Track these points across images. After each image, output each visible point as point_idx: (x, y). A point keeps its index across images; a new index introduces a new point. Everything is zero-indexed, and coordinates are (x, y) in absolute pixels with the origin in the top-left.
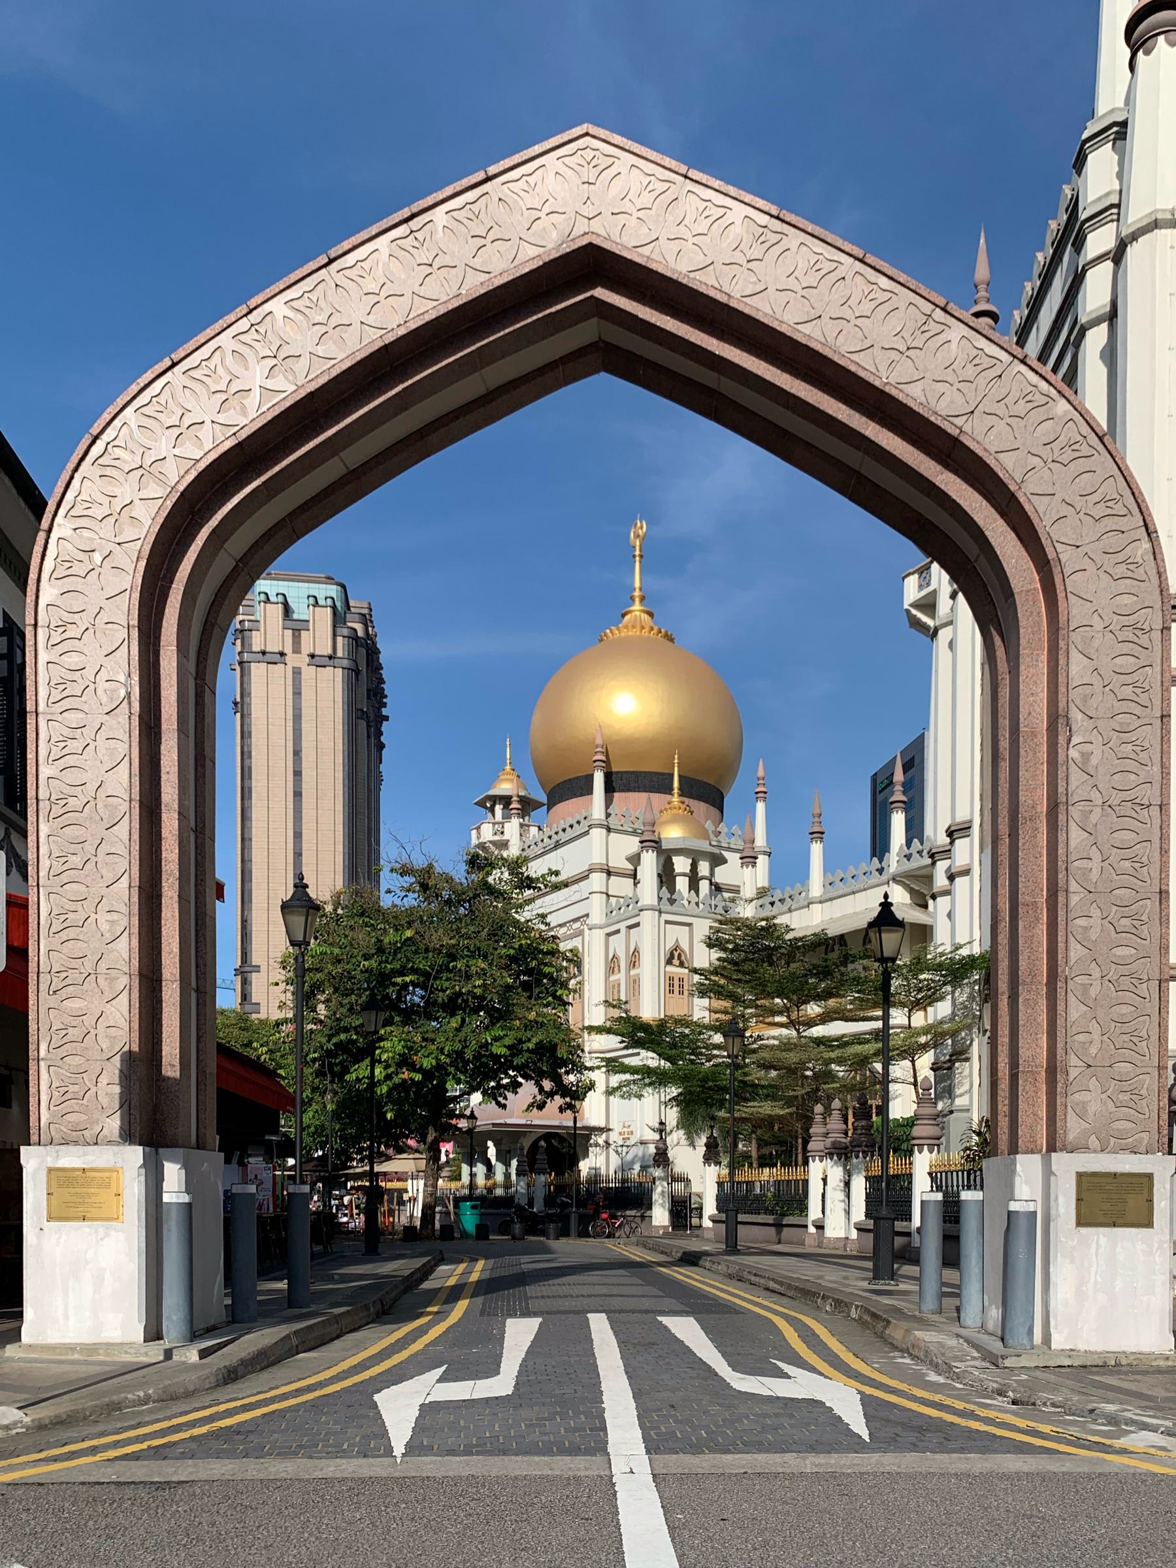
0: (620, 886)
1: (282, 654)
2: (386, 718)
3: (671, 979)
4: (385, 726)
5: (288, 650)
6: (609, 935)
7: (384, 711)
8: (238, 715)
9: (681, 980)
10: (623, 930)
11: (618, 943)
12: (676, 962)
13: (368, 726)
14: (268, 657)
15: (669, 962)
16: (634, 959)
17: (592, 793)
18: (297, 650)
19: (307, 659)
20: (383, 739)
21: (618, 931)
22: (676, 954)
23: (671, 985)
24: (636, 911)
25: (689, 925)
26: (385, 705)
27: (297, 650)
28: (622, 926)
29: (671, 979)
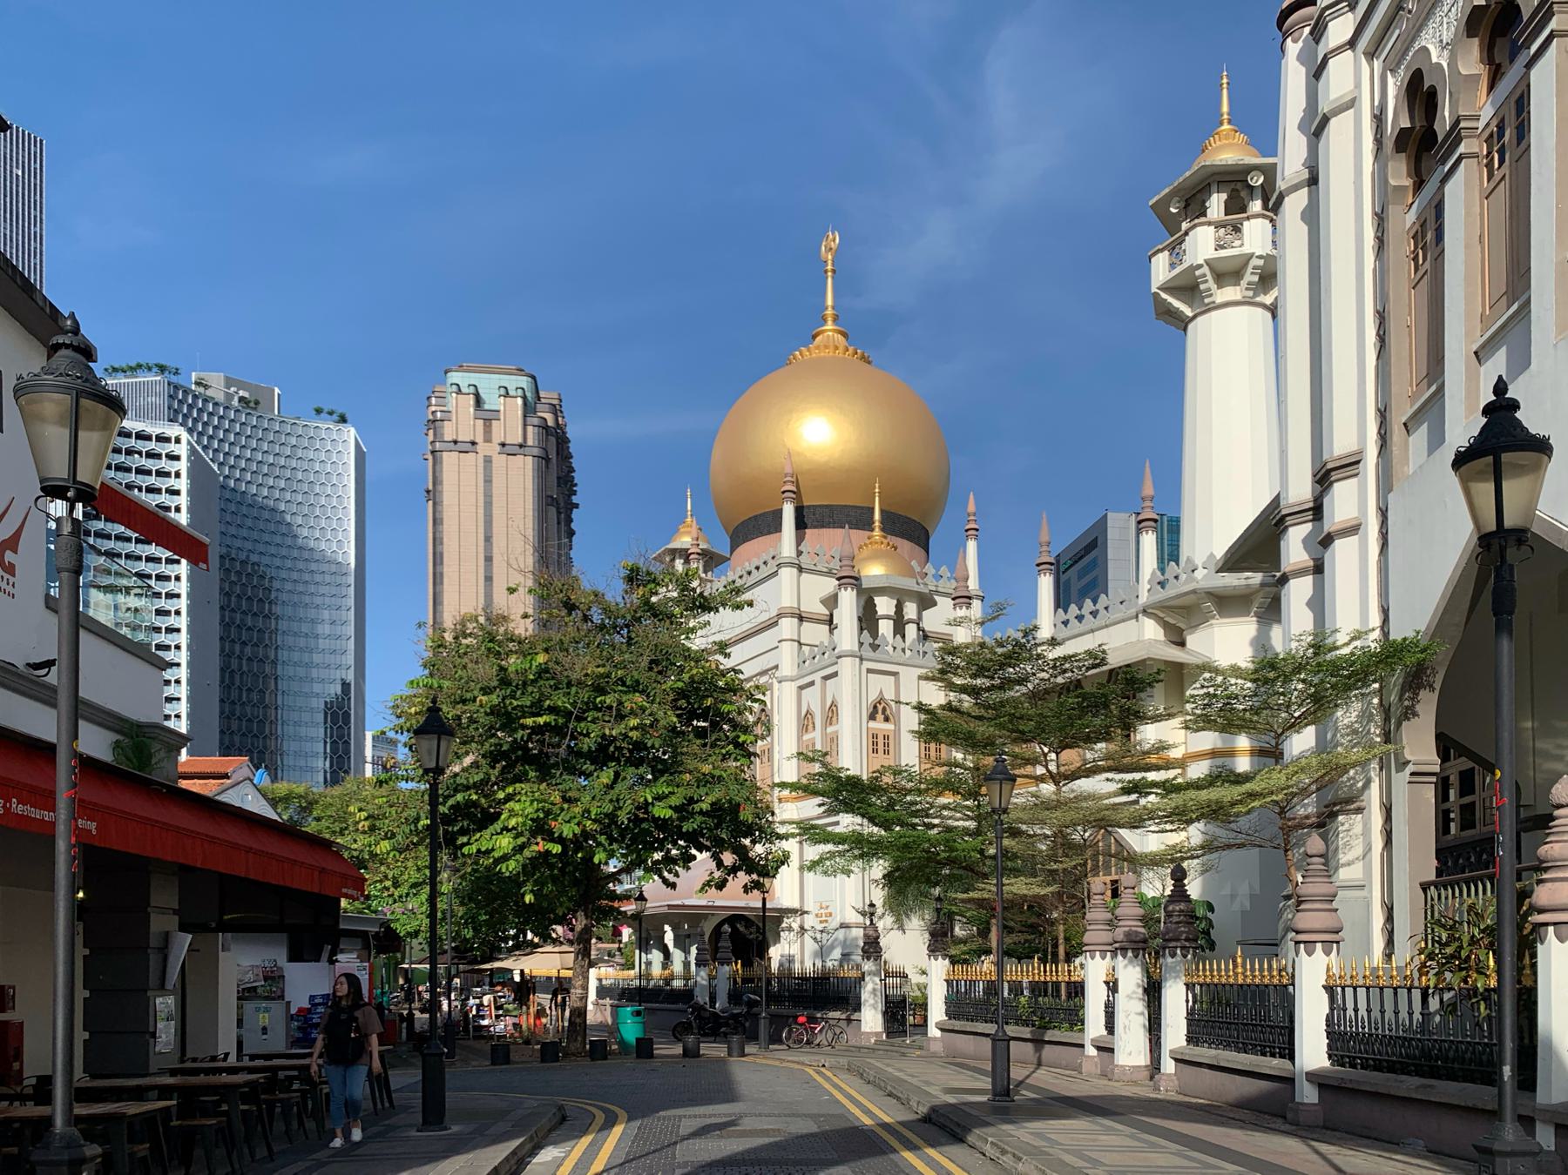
0: (815, 633)
1: (473, 443)
2: (577, 506)
3: (875, 736)
4: (575, 514)
5: (479, 439)
6: (801, 688)
7: (575, 499)
8: (431, 502)
9: (886, 737)
10: (818, 682)
11: (812, 698)
12: (880, 716)
13: (559, 513)
14: (460, 447)
15: (872, 717)
16: (832, 713)
17: (780, 531)
18: (488, 440)
19: (498, 448)
20: (573, 526)
21: (812, 683)
22: (880, 708)
23: (875, 744)
24: (834, 659)
25: (895, 674)
26: (575, 493)
27: (488, 440)
28: (817, 677)
29: (875, 736)
